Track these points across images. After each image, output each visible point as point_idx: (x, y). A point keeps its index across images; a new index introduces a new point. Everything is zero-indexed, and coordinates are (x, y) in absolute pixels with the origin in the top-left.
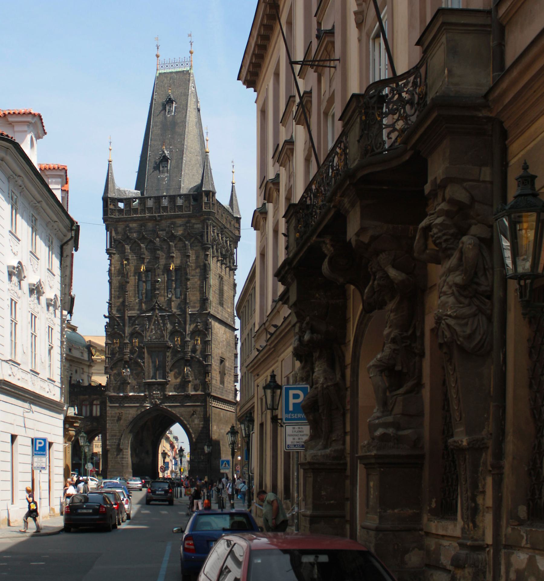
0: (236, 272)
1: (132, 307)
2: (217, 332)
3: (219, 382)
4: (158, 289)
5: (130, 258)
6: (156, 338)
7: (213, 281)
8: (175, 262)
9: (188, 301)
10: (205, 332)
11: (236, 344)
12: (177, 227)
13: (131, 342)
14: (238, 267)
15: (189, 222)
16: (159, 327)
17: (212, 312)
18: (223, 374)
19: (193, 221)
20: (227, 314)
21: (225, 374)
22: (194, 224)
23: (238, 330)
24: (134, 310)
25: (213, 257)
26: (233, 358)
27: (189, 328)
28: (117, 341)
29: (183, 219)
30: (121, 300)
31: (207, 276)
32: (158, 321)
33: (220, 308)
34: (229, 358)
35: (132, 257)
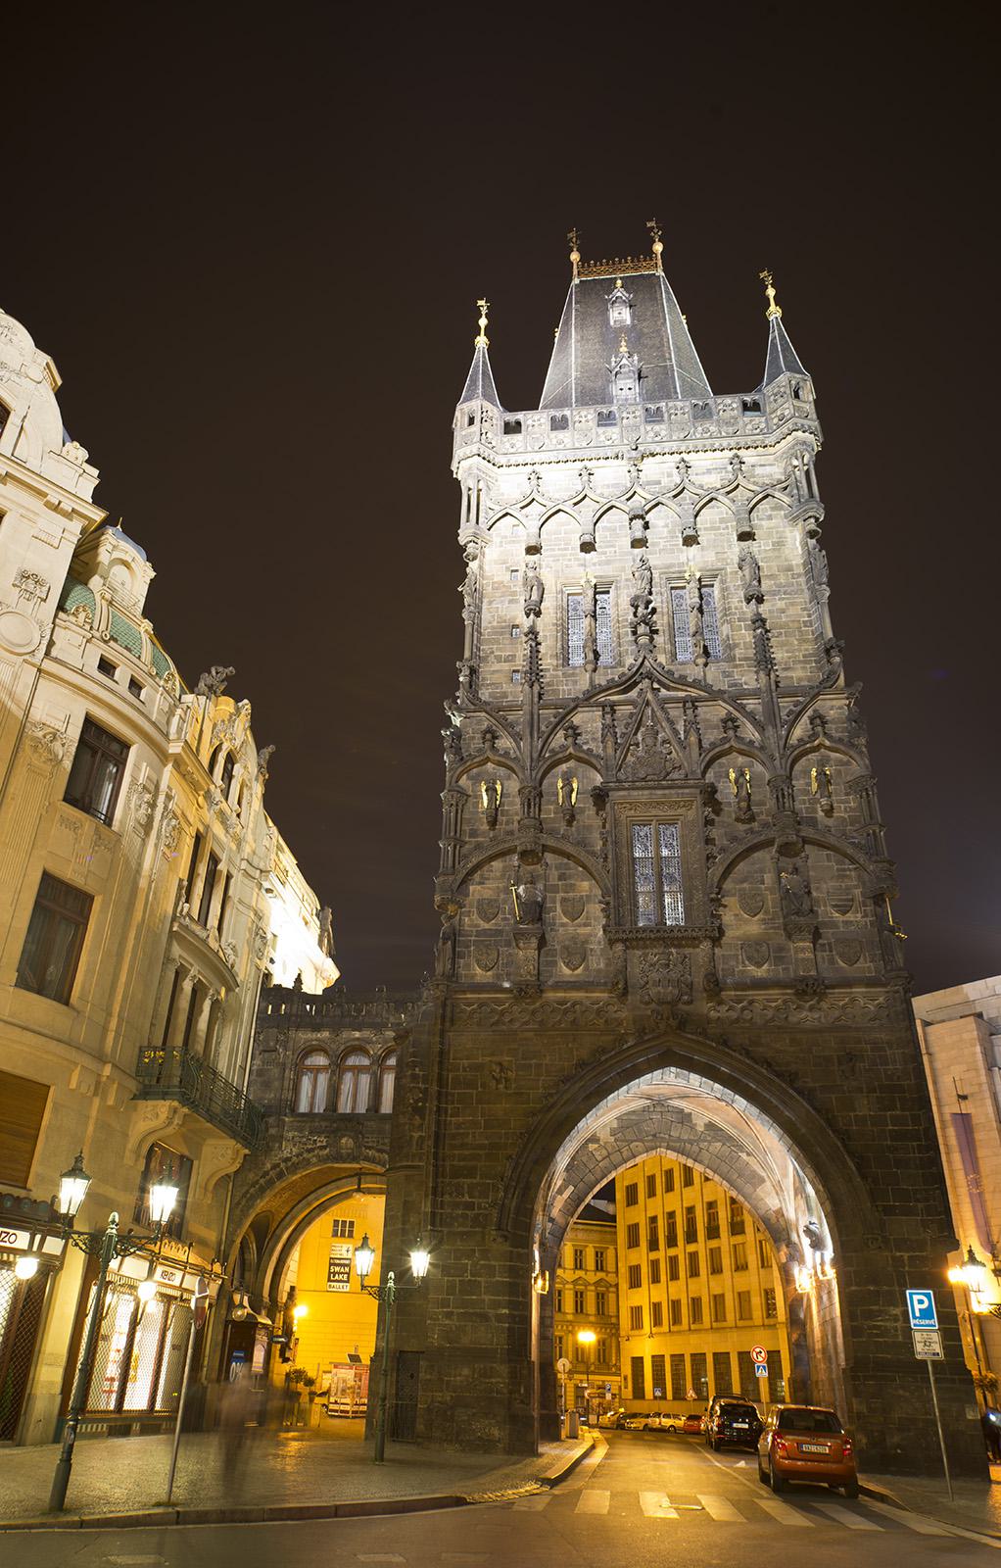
1: (548, 684)
12: (697, 474)
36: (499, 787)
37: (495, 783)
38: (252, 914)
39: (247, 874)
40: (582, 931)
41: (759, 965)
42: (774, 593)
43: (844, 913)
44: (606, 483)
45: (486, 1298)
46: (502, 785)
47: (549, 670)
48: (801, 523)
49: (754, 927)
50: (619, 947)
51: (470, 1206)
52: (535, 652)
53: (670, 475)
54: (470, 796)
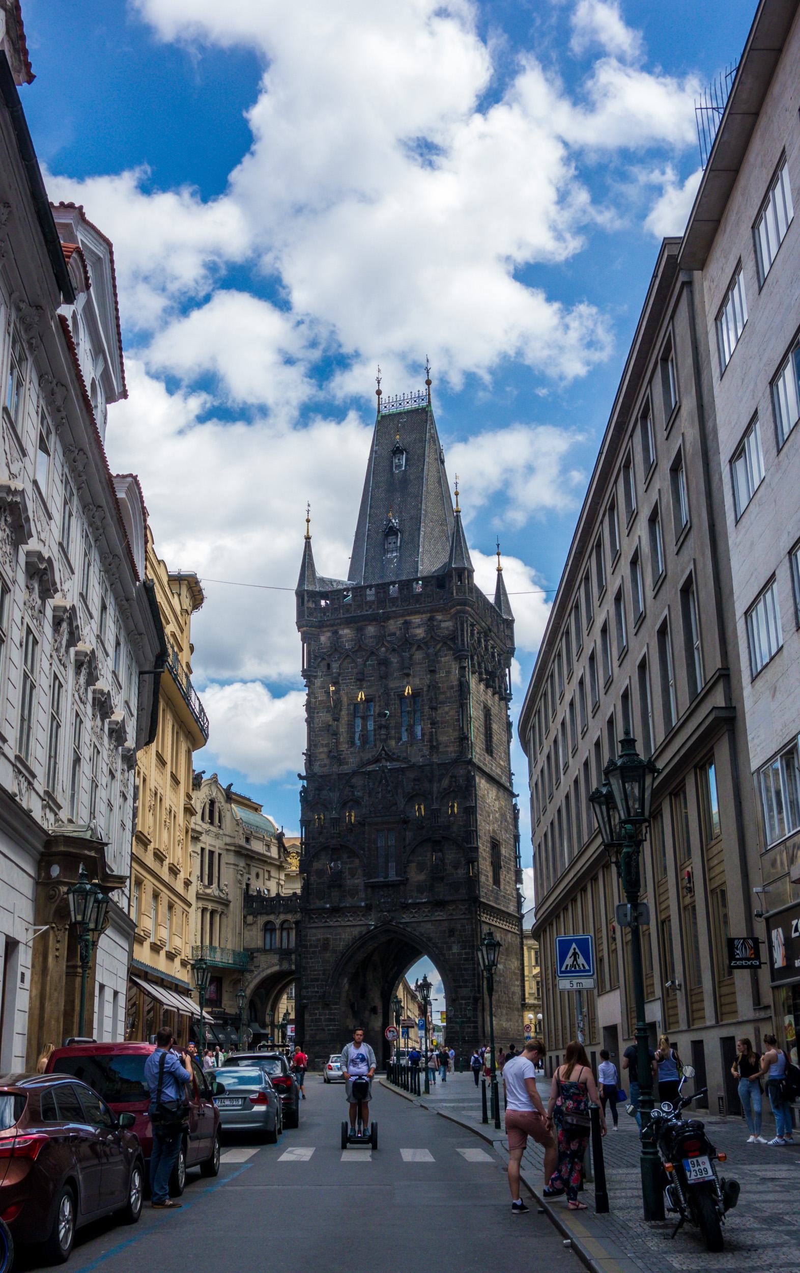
0: (510, 704)
1: (344, 759)
2: (484, 795)
3: (491, 880)
5: (341, 682)
7: (475, 712)
8: (411, 682)
11: (516, 818)
14: (513, 697)
15: (431, 619)
17: (475, 760)
18: (496, 866)
19: (439, 617)
20: (499, 769)
21: (501, 868)
22: (440, 621)
26: (512, 842)
29: (424, 616)
33: (488, 758)
34: (505, 841)
36: (322, 817)
37: (319, 815)
38: (232, 866)
39: (227, 850)
40: (356, 881)
41: (422, 894)
42: (443, 703)
43: (456, 869)
47: (343, 751)
49: (422, 877)
50: (370, 890)
51: (317, 992)
52: (337, 743)
53: (401, 629)
54: (310, 821)
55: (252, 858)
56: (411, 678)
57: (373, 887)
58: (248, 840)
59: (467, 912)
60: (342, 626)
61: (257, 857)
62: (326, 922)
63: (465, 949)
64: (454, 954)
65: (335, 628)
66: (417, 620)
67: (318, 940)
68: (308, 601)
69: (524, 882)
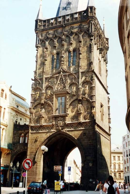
1: (48, 73)
4: (63, 61)
5: (48, 48)
6: (61, 89)
9: (80, 65)
10: (91, 82)
13: (46, 93)
16: (63, 82)
19: (84, 24)
21: (104, 115)
22: (84, 26)
23: (109, 94)
24: (49, 75)
25: (95, 44)
27: (81, 80)
28: (38, 93)
29: (78, 24)
30: (41, 70)
31: (92, 50)
32: (62, 78)
35: (49, 47)
41: (74, 119)
44: (59, 32)
45: (34, 169)
46: (40, 92)
48: (90, 38)
50: (54, 118)
55: (19, 113)
56: (73, 44)
57: (56, 118)
58: (18, 106)
59: (91, 126)
60: (50, 30)
61: (20, 112)
62: (38, 131)
63: (90, 141)
64: (85, 143)
65: (48, 31)
66: (75, 26)
67: (34, 137)
68: (39, 23)
69: (111, 123)
